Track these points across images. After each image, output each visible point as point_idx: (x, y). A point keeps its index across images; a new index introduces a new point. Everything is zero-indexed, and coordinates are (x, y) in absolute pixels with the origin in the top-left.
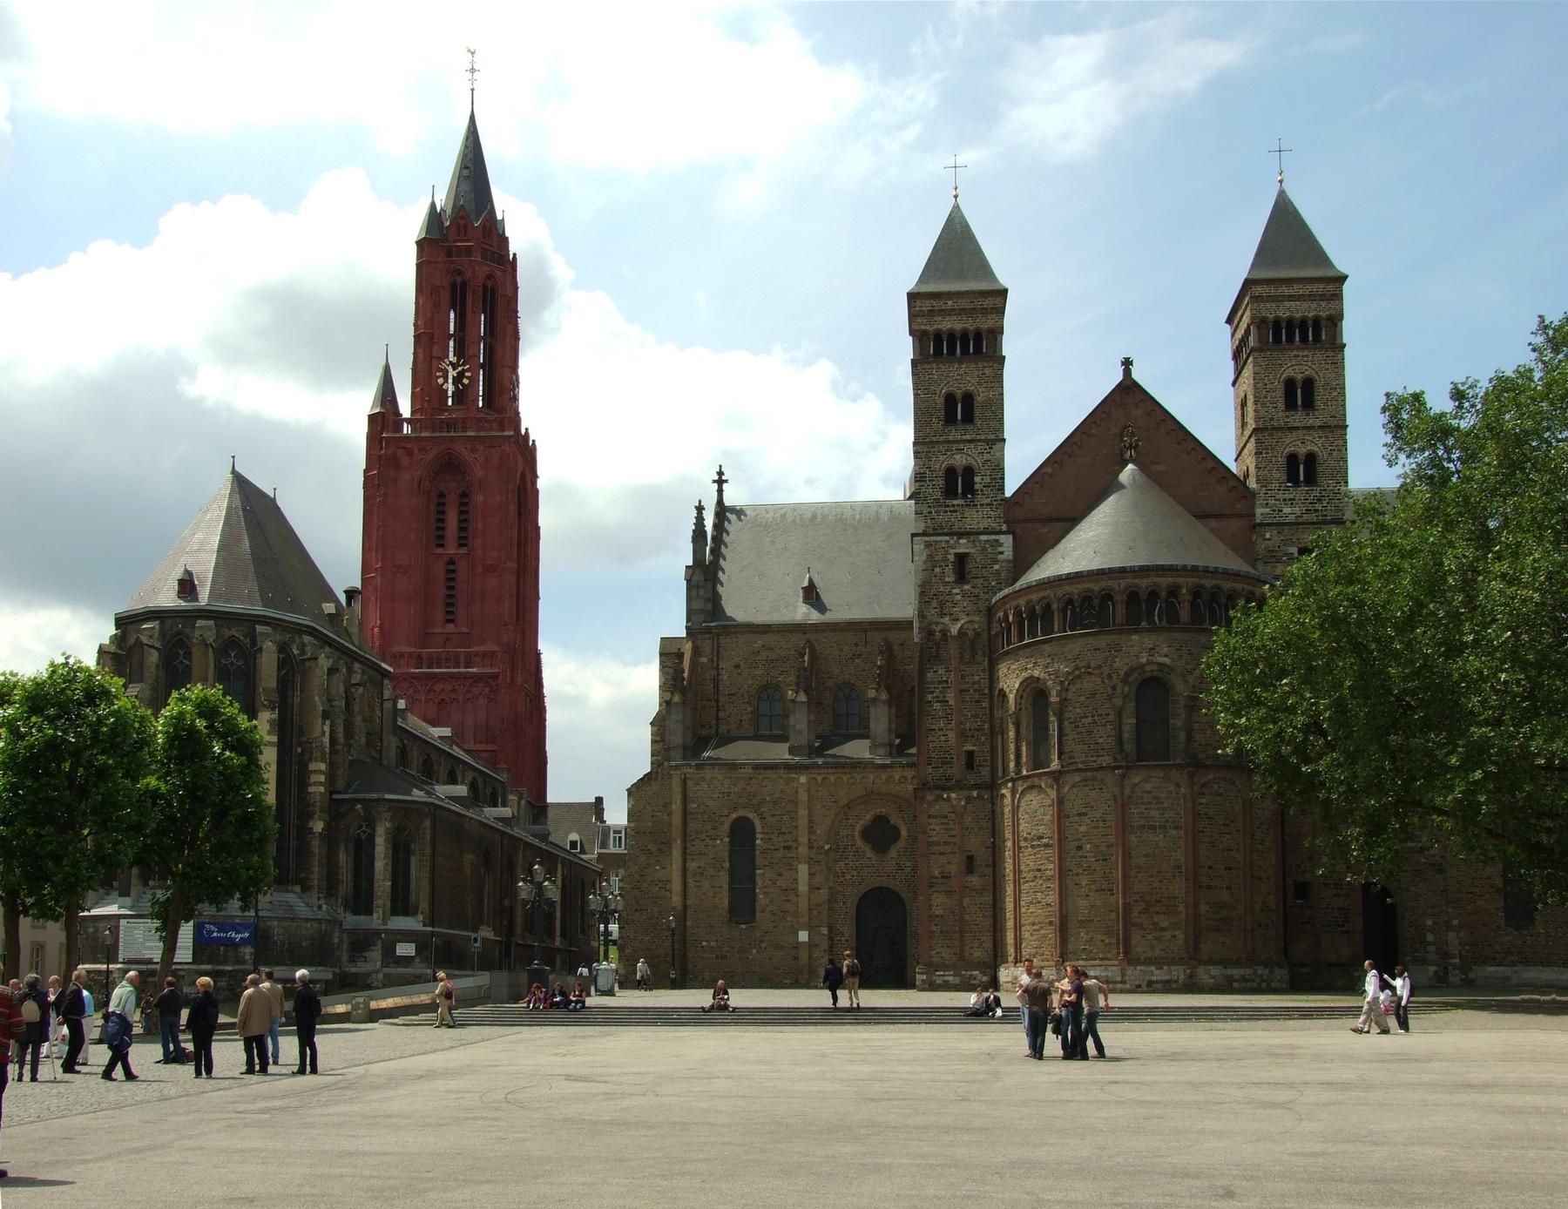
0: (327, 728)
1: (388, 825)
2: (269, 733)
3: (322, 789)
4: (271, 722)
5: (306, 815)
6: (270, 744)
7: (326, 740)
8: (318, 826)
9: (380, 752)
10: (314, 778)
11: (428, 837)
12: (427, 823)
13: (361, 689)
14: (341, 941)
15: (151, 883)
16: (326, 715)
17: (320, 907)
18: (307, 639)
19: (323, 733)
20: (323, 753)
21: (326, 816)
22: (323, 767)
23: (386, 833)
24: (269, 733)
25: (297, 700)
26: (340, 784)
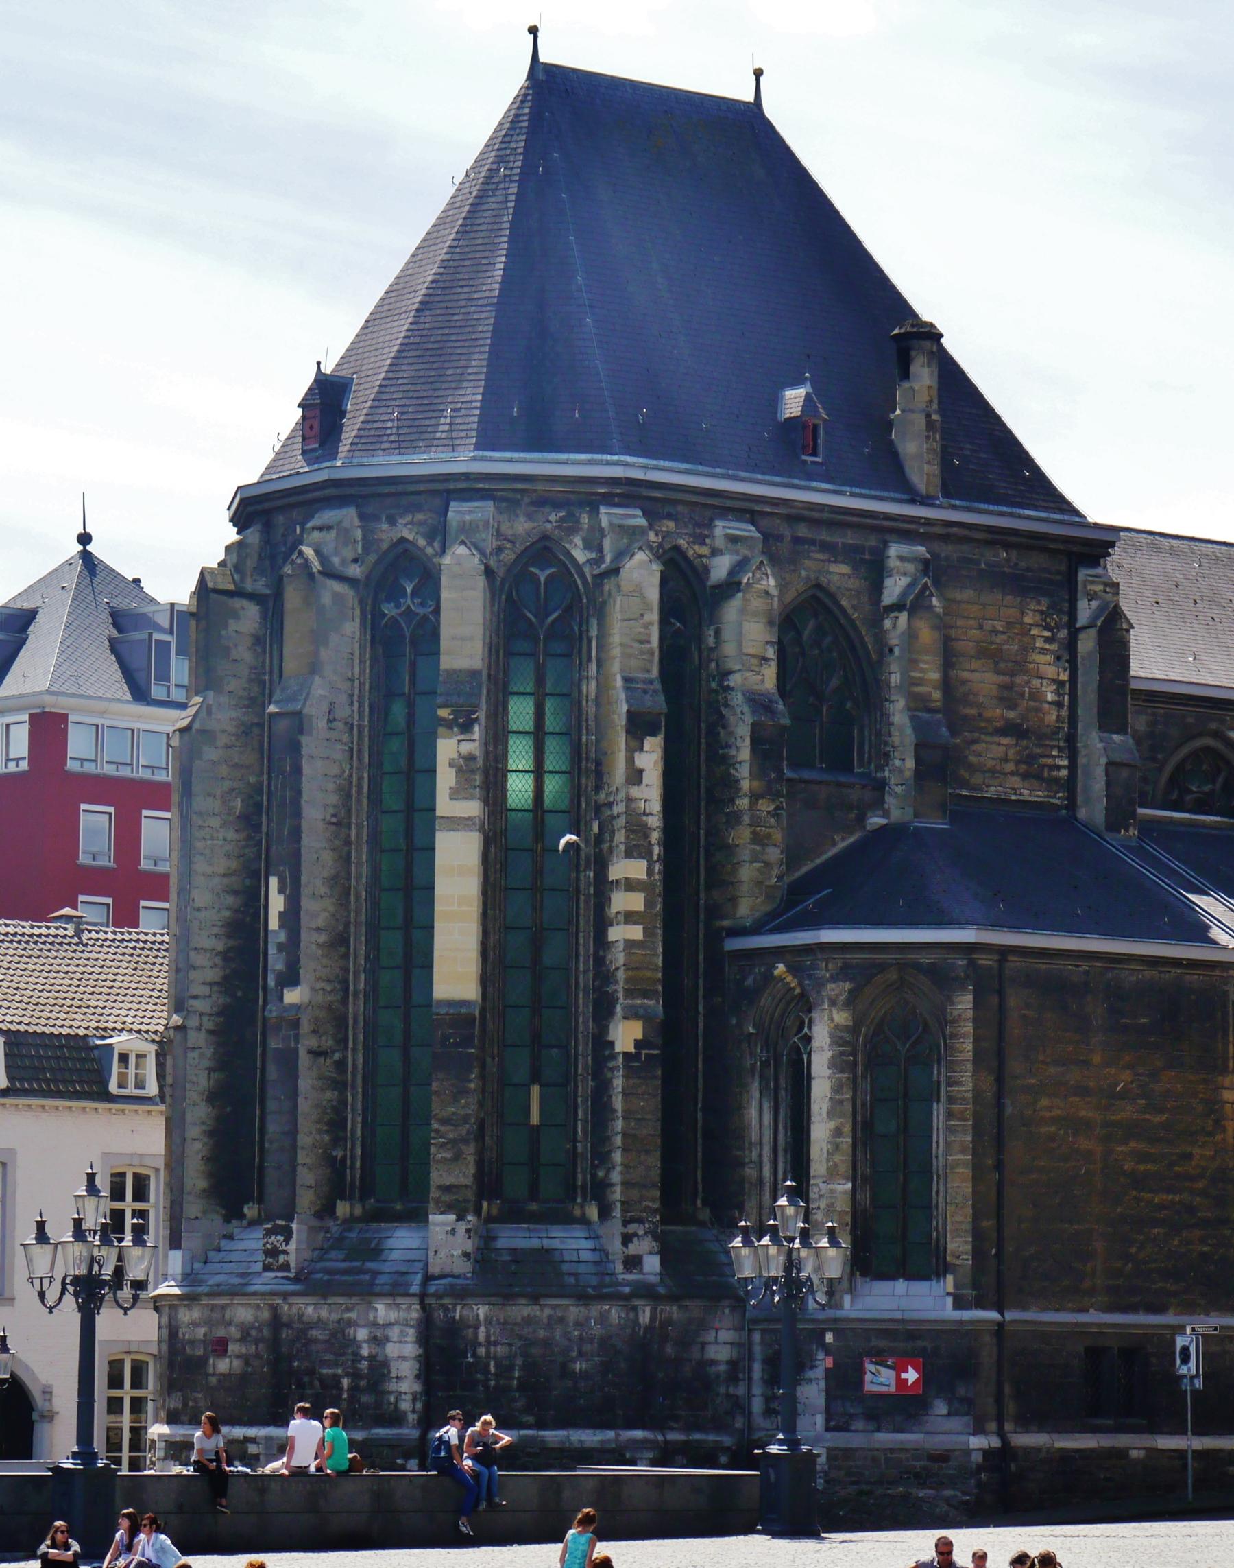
0: (650, 758)
1: (841, 1017)
2: (455, 795)
3: (636, 932)
4: (464, 766)
5: (603, 1010)
6: (456, 823)
7: (650, 795)
8: (626, 1035)
9: (1070, 785)
10: (621, 902)
11: (966, 1048)
12: (964, 1003)
13: (903, 617)
14: (744, 1350)
15: (250, 1211)
16: (639, 727)
17: (633, 1263)
18: (607, 515)
19: (636, 776)
20: (637, 828)
21: (655, 1006)
22: (636, 869)
23: (843, 1040)
24: (455, 795)
25: (590, 689)
26: (747, 908)
